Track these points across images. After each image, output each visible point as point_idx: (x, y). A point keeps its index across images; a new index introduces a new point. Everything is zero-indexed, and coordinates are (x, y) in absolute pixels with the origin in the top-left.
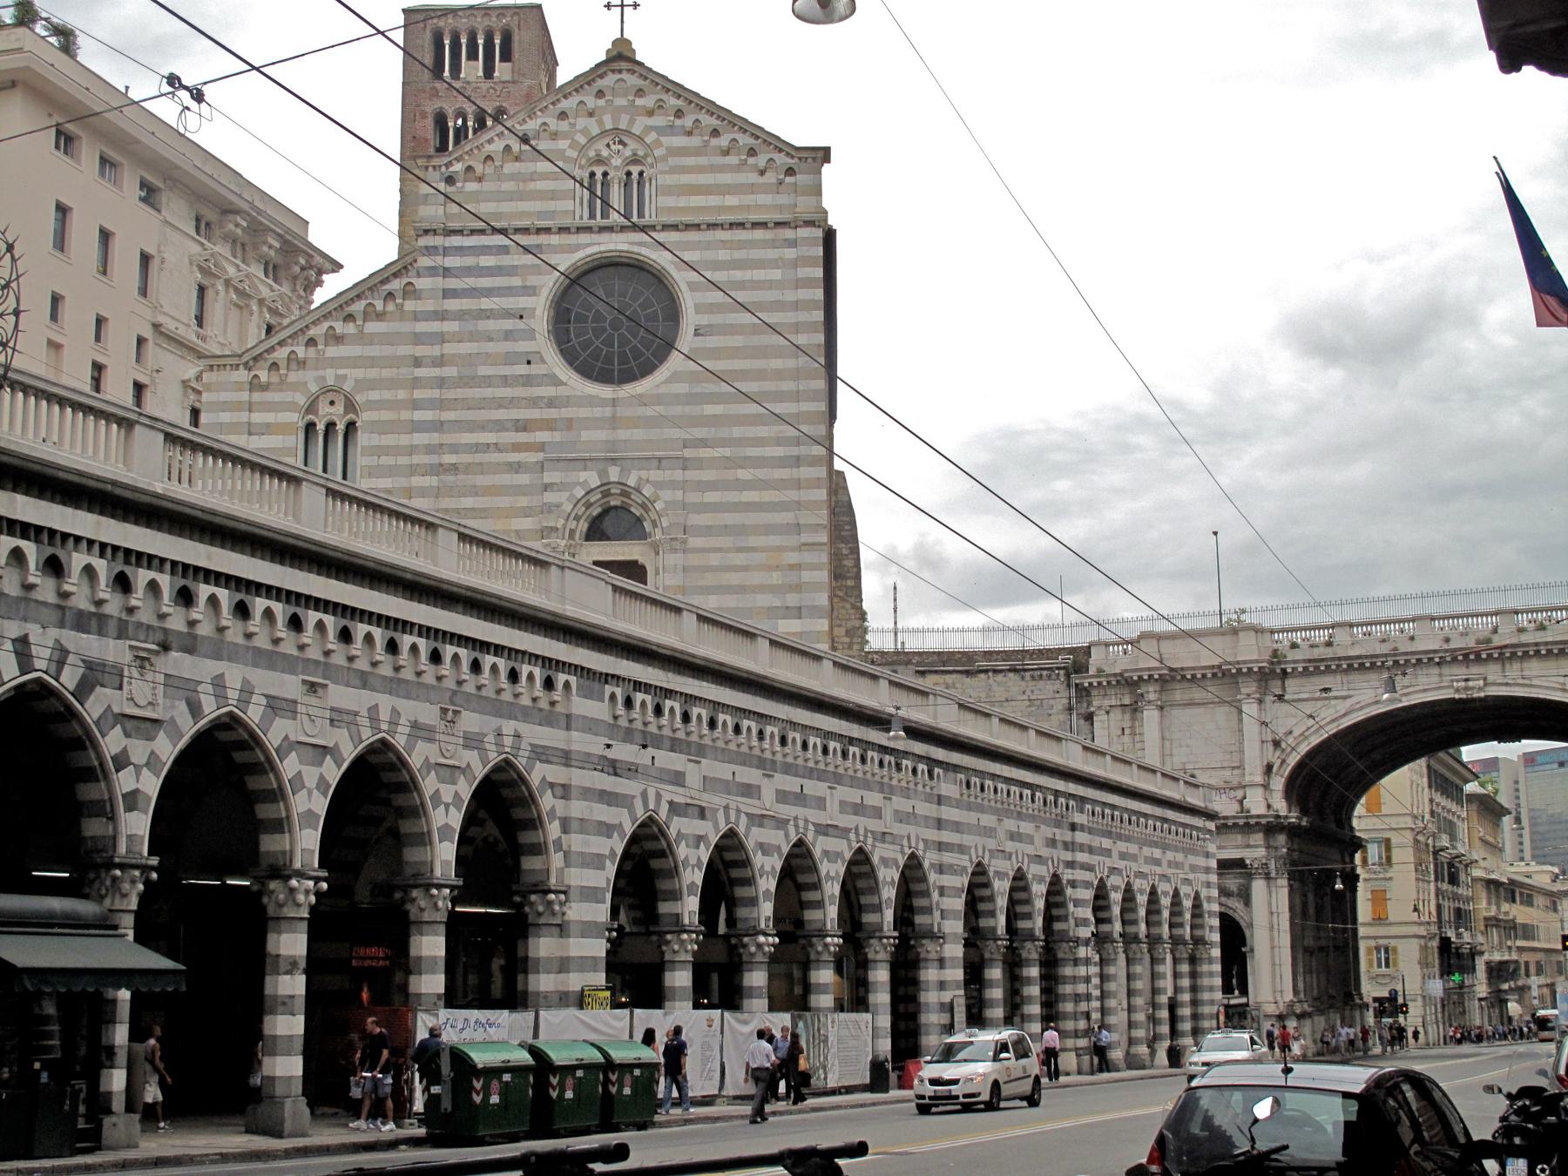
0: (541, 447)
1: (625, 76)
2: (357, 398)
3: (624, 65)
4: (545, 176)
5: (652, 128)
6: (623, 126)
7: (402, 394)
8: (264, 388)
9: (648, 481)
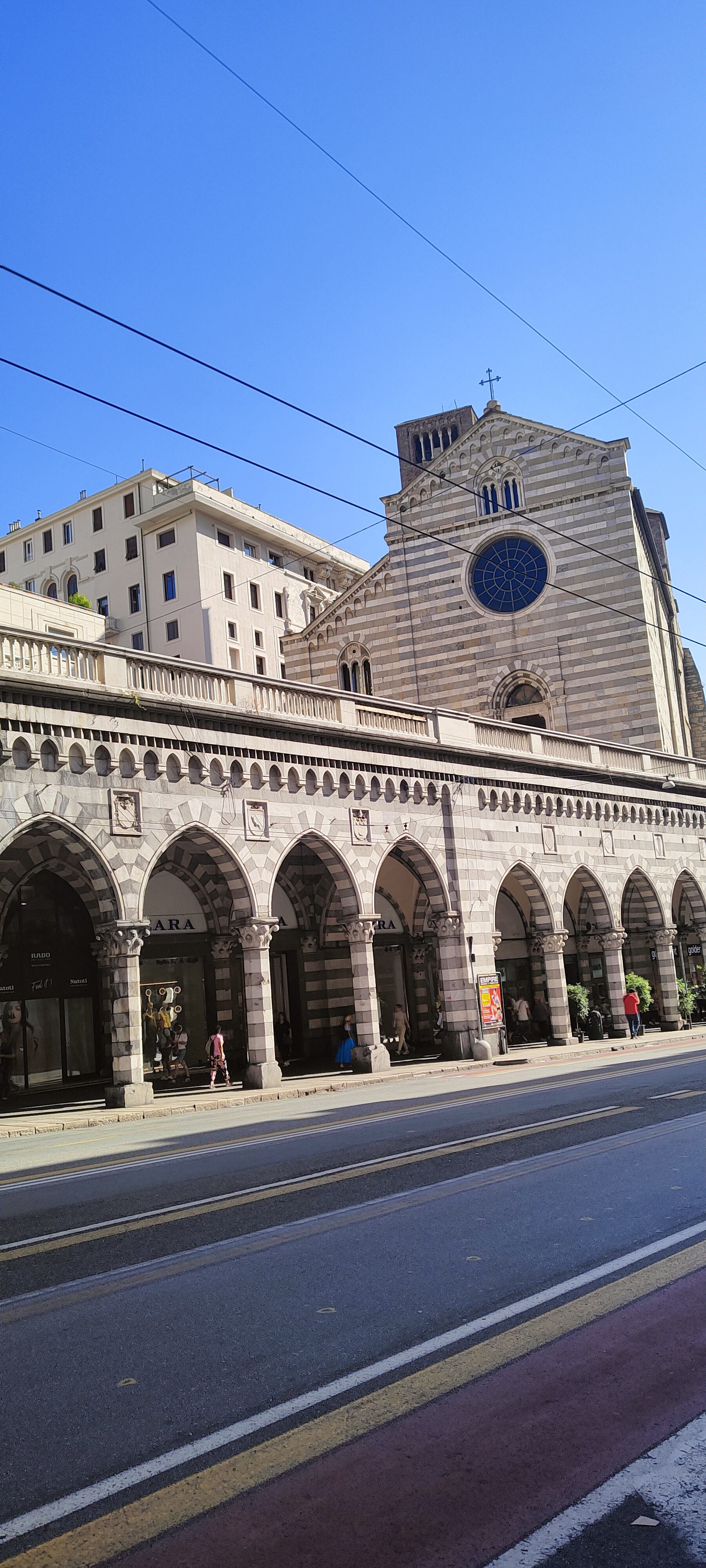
0: (474, 656)
3: (495, 416)
4: (456, 495)
5: (517, 451)
7: (391, 640)
9: (538, 665)
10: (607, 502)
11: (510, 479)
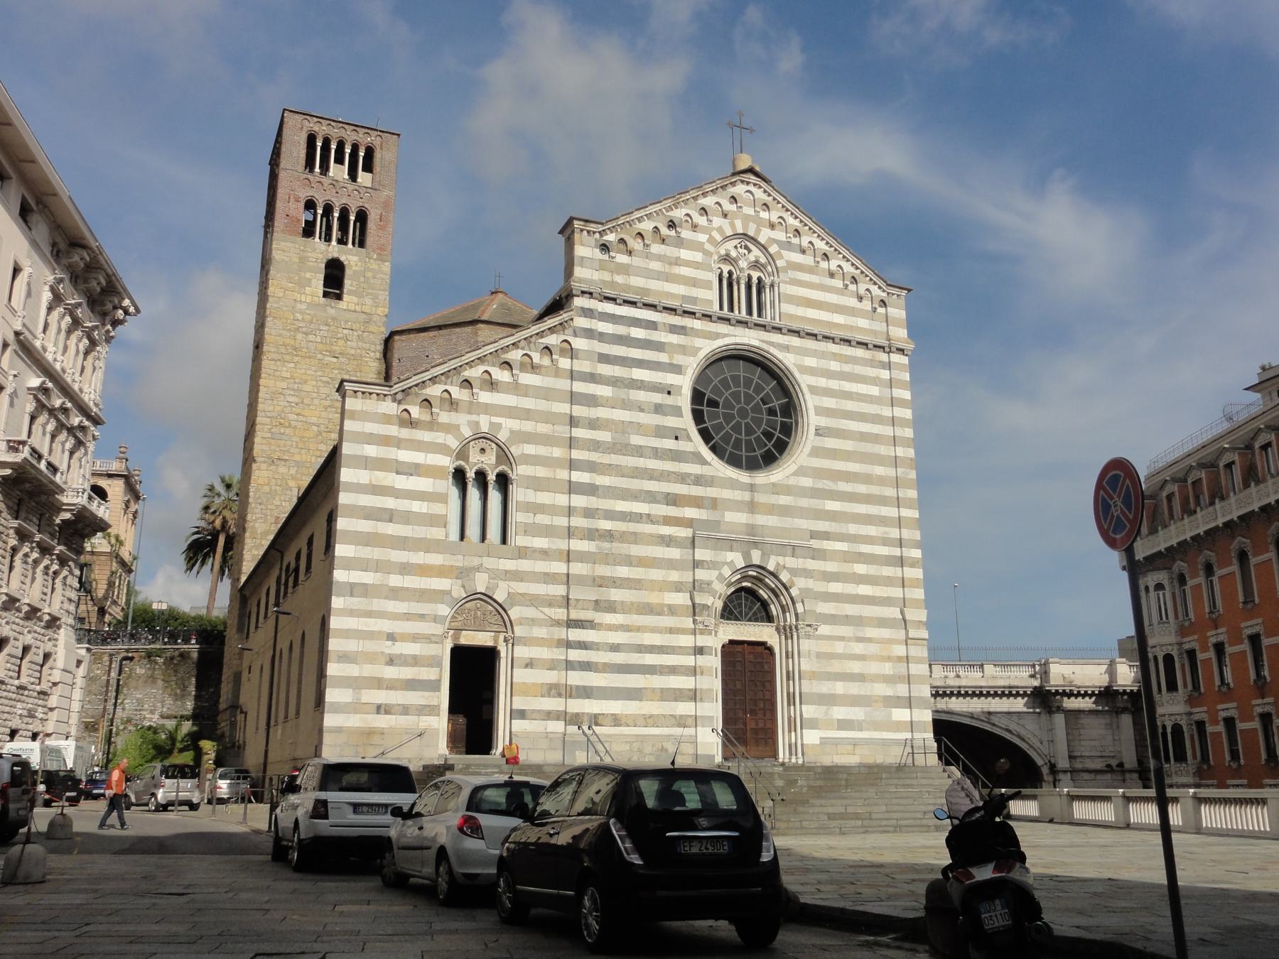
0: (689, 523)
1: (751, 188)
2: (513, 449)
3: (753, 178)
6: (751, 233)
7: (557, 452)
8: (411, 423)
10: (880, 362)
11: (755, 275)
